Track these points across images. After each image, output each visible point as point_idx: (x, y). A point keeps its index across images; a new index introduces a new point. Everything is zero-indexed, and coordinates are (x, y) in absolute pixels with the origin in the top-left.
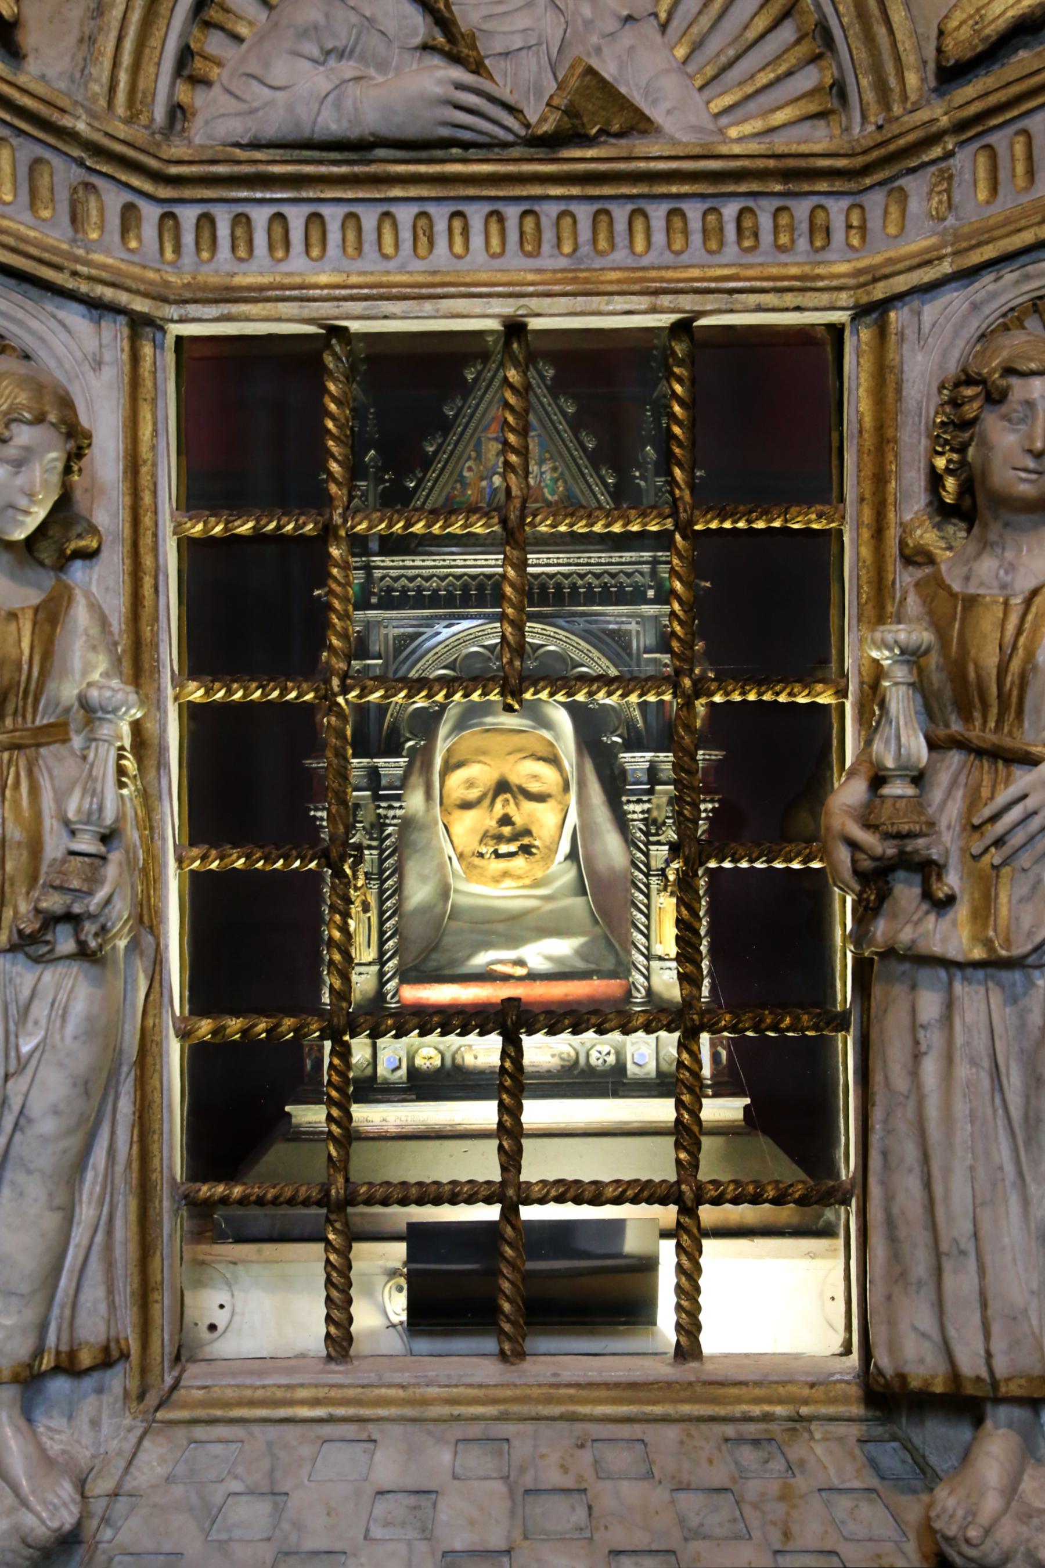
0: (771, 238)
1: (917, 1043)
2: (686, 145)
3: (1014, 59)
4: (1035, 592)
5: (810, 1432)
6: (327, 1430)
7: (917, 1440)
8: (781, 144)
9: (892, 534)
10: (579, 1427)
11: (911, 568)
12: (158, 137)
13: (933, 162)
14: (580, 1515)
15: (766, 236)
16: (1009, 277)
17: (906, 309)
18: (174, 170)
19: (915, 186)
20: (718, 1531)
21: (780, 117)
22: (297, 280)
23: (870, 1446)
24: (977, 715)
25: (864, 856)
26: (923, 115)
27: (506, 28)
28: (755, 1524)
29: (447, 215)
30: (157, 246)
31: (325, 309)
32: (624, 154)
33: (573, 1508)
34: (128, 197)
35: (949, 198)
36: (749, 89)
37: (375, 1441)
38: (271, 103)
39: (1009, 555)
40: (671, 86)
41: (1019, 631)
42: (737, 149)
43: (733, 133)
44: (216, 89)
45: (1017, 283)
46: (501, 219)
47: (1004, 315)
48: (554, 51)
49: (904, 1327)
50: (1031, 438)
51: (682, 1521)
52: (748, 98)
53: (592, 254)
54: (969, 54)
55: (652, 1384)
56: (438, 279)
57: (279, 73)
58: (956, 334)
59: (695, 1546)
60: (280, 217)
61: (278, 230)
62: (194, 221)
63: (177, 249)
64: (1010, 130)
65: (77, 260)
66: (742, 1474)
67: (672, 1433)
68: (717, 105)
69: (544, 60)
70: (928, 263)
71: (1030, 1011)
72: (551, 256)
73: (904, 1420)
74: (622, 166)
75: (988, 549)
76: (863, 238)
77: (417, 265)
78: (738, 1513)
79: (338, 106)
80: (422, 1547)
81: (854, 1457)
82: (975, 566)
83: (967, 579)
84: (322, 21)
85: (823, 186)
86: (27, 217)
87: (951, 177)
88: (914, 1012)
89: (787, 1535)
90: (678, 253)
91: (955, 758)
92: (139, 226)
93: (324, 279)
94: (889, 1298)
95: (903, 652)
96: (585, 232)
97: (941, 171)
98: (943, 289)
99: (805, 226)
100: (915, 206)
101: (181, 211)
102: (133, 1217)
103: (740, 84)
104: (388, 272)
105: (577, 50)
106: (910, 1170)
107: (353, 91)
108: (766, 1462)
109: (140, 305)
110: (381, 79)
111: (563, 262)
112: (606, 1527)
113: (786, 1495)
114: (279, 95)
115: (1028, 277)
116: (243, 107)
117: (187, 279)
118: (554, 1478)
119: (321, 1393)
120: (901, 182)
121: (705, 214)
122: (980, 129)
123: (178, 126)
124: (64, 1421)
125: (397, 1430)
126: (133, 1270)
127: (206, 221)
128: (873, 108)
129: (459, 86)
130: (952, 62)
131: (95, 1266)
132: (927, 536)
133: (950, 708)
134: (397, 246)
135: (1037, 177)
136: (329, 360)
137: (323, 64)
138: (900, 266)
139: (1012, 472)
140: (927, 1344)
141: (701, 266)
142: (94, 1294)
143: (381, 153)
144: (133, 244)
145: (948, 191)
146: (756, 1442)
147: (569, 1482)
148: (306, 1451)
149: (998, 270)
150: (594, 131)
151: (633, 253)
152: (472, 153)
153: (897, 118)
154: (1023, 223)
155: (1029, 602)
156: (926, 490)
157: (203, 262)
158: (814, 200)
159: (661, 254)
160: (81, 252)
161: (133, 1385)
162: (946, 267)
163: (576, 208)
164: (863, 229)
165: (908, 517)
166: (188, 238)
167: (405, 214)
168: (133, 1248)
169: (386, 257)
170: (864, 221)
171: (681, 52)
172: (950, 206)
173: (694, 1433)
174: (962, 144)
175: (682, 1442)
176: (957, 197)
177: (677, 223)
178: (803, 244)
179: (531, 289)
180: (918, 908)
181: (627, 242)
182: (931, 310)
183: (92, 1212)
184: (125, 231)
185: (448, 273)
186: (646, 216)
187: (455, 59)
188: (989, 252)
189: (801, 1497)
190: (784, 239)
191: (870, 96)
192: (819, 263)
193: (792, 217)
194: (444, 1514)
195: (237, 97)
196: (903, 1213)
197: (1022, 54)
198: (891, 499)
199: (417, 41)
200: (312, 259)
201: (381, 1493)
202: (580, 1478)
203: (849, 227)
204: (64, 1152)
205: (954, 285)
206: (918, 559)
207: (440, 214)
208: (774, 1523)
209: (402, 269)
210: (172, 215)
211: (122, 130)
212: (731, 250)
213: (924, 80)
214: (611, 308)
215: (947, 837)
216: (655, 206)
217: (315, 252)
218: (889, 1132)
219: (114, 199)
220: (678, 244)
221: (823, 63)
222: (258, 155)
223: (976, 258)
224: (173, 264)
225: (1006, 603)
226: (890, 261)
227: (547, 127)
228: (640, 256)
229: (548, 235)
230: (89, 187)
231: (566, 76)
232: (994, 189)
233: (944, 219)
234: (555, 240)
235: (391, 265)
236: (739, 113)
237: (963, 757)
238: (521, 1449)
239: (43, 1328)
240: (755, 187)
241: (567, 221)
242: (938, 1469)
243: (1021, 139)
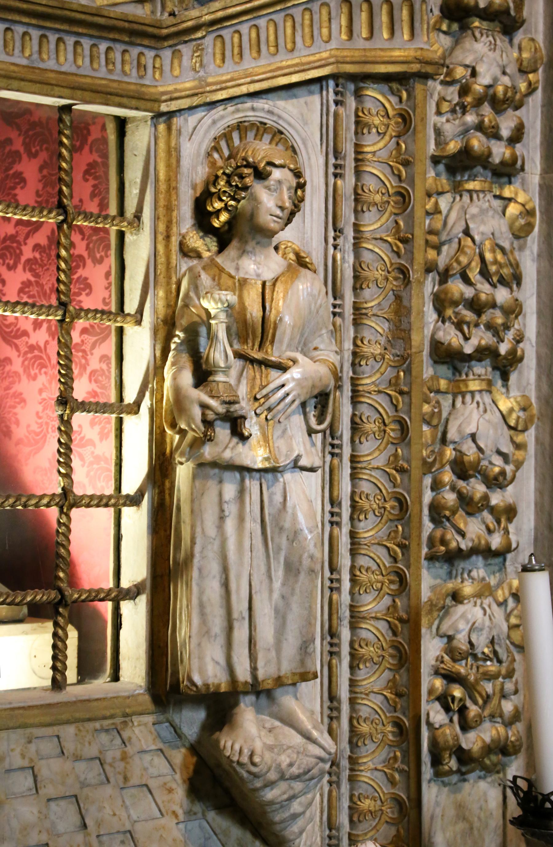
1: (222, 511)
7: (177, 721)
10: (28, 731)
11: (185, 259)
16: (230, 109)
17: (182, 118)
19: (186, 50)
20: (93, 781)
23: (156, 726)
24: (250, 341)
25: (211, 413)
28: (111, 775)
29: (4, 29)
32: (60, 6)
33: (26, 778)
35: (201, 61)
45: (233, 112)
49: (208, 659)
53: (39, 60)
55: (58, 704)
59: (85, 790)
64: (232, 30)
67: (71, 730)
70: (196, 95)
71: (275, 494)
72: (19, 57)
73: (171, 711)
74: (59, 12)
75: (245, 254)
76: (161, 74)
78: (102, 771)
81: (151, 732)
82: (240, 262)
85: (146, 42)
88: (220, 495)
89: (126, 779)
94: (199, 645)
95: (228, 306)
97: (199, 45)
98: (197, 109)
106: (214, 577)
108: (112, 741)
112: (45, 786)
113: (124, 758)
115: (238, 111)
120: (179, 47)
122: (219, 26)
133: (234, 337)
135: (244, 57)
138: (183, 94)
139: (270, 217)
140: (218, 667)
146: (107, 731)
149: (226, 104)
154: (242, 81)
156: (192, 217)
159: (71, 66)
164: (161, 69)
165: (184, 231)
172: (201, 65)
173: (81, 728)
174: (208, 33)
175: (76, 735)
176: (205, 61)
180: (230, 439)
181: (55, 56)
182: (193, 119)
189: (130, 757)
196: (209, 600)
198: (174, 220)
202: (31, 760)
205: (203, 108)
206: (191, 254)
208: (119, 773)
215: (243, 404)
216: (68, 38)
218: (203, 558)
220: (95, 66)
226: (176, 90)
229: (18, 44)
233: (199, 72)
234: (21, 48)
237: (241, 363)
240: (117, 36)
242: (187, 734)
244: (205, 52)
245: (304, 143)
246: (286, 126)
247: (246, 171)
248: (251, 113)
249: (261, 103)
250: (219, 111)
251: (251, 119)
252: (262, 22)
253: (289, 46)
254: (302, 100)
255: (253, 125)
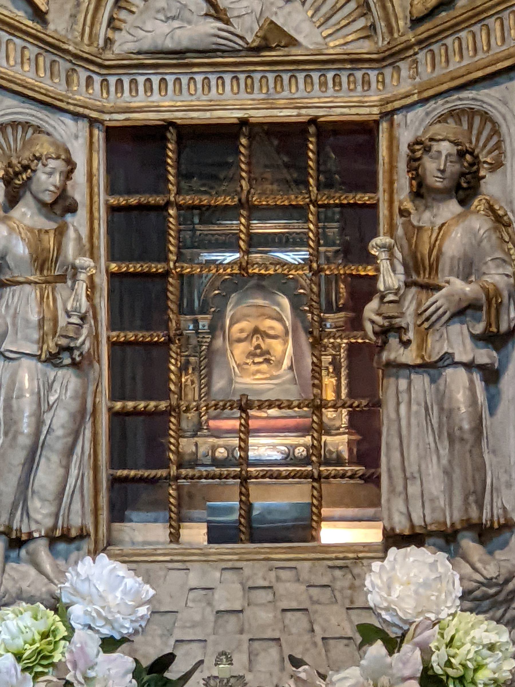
0: (346, 86)
2: (311, 50)
3: (441, 15)
4: (443, 225)
5: (362, 563)
6: (170, 565)
8: (349, 48)
9: (396, 204)
12: (101, 51)
13: (411, 56)
14: (270, 597)
15: (345, 85)
16: (440, 102)
18: (107, 63)
21: (350, 38)
22: (155, 104)
24: (422, 272)
26: (404, 38)
27: (239, 7)
30: (100, 92)
31: (167, 116)
34: (89, 73)
36: (338, 27)
37: (189, 569)
38: (145, 37)
39: (435, 210)
40: (306, 27)
41: (436, 240)
42: (331, 51)
43: (332, 44)
44: (124, 33)
45: (443, 105)
46: (237, 79)
47: (439, 117)
48: (258, 16)
50: (440, 165)
51: (311, 598)
52: (338, 30)
54: (422, 15)
56: (212, 103)
57: (149, 26)
58: (420, 124)
60: (149, 80)
61: (148, 84)
62: (115, 82)
63: (108, 93)
64: (440, 44)
65: (70, 98)
66: (334, 579)
67: (307, 564)
68: (324, 34)
69: (254, 17)
77: (204, 98)
79: (172, 38)
80: (208, 610)
83: (419, 221)
84: (165, 6)
85: (366, 66)
86: (49, 82)
87: (417, 62)
89: (352, 602)
90: (309, 92)
91: (413, 290)
92: (93, 84)
93: (167, 104)
96: (271, 84)
99: (360, 81)
100: (404, 73)
101: (109, 78)
102: (91, 479)
103: (335, 25)
104: (192, 101)
105: (266, 14)
107: (178, 32)
109: (94, 115)
110: (189, 27)
111: (262, 96)
114: (149, 34)
115: (447, 102)
116: (135, 39)
117: (112, 105)
118: (261, 583)
119: (167, 551)
120: (397, 64)
121: (320, 76)
123: (109, 46)
124: (64, 562)
125: (197, 565)
126: (92, 500)
127: (120, 82)
128: (386, 35)
129: (220, 29)
130: (415, 17)
131: (77, 497)
132: (408, 205)
134: (196, 90)
136: (169, 136)
137: (166, 22)
141: (319, 98)
142: (76, 506)
143: (188, 55)
144: (91, 91)
145: (417, 68)
146: (340, 568)
147: (266, 584)
148: (162, 573)
150: (274, 45)
151: (291, 92)
152: (226, 54)
153: (396, 39)
155: (440, 229)
157: (118, 98)
158: (364, 71)
160: (70, 95)
161: (92, 547)
162: (415, 98)
163: (268, 75)
164: (383, 82)
165: (402, 197)
166: (112, 89)
167: (199, 78)
168: (92, 493)
169: (191, 95)
170: (384, 79)
171: (310, 13)
174: (421, 49)
177: (309, 80)
178: (359, 88)
179: (250, 107)
182: (410, 115)
183: (76, 471)
184: (87, 86)
185: (217, 101)
186: (296, 77)
187: (218, 19)
188: (431, 92)
190: (352, 86)
191: (385, 30)
192: (365, 96)
193: (355, 77)
194: (216, 596)
195: (132, 35)
197: (444, 14)
198: (395, 191)
199: (203, 13)
200: (161, 96)
201: (191, 589)
202: (270, 582)
203: (378, 81)
204: (66, 444)
205: (419, 105)
207: (213, 78)
209: (198, 100)
210: (106, 80)
211: (87, 49)
212: (331, 91)
213: (406, 24)
214: (282, 114)
217: (163, 93)
219: (83, 75)
221: (367, 16)
222: (140, 57)
223: (426, 95)
224: (106, 99)
225: (432, 229)
227: (255, 44)
228: (294, 94)
230: (73, 70)
231: (262, 25)
232: (434, 67)
233: (415, 79)
235: (193, 98)
236: (334, 37)
238: (247, 571)
239: (57, 516)
241: (264, 81)
243: (444, 47)
244: (419, 64)
245: (505, 119)
246: (489, 108)
247: (417, 147)
248: (459, 103)
249: (465, 94)
250: (431, 104)
251: (461, 107)
252: (463, 34)
253: (485, 48)
254: (503, 86)
255: (463, 110)
